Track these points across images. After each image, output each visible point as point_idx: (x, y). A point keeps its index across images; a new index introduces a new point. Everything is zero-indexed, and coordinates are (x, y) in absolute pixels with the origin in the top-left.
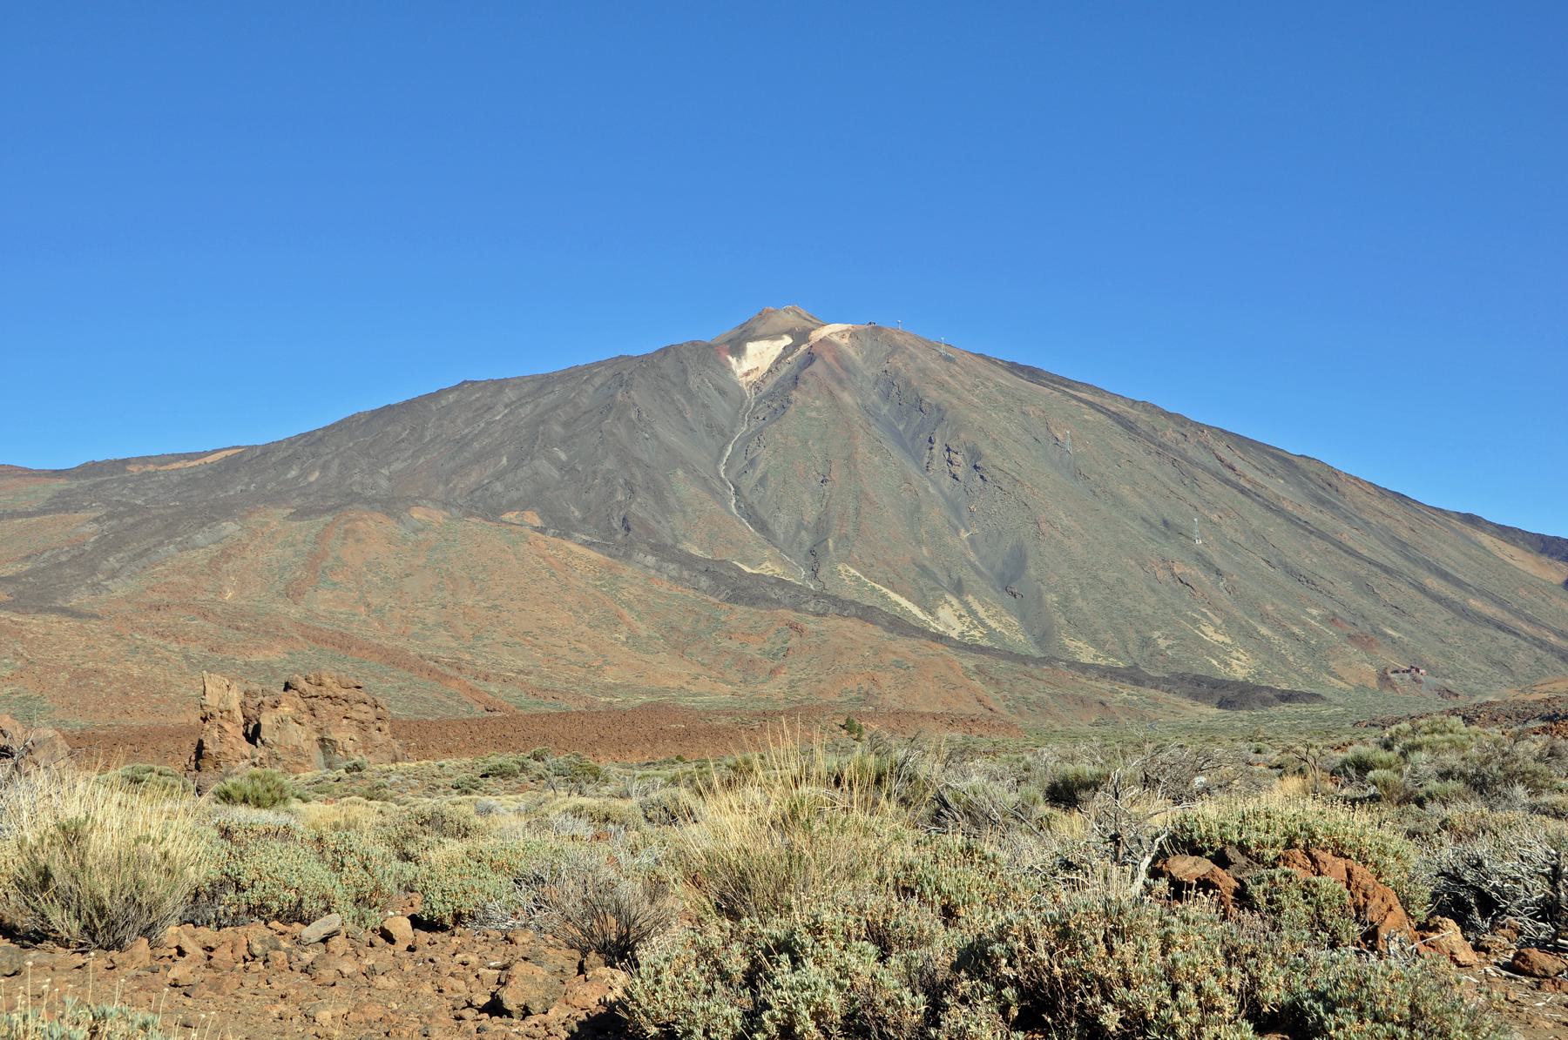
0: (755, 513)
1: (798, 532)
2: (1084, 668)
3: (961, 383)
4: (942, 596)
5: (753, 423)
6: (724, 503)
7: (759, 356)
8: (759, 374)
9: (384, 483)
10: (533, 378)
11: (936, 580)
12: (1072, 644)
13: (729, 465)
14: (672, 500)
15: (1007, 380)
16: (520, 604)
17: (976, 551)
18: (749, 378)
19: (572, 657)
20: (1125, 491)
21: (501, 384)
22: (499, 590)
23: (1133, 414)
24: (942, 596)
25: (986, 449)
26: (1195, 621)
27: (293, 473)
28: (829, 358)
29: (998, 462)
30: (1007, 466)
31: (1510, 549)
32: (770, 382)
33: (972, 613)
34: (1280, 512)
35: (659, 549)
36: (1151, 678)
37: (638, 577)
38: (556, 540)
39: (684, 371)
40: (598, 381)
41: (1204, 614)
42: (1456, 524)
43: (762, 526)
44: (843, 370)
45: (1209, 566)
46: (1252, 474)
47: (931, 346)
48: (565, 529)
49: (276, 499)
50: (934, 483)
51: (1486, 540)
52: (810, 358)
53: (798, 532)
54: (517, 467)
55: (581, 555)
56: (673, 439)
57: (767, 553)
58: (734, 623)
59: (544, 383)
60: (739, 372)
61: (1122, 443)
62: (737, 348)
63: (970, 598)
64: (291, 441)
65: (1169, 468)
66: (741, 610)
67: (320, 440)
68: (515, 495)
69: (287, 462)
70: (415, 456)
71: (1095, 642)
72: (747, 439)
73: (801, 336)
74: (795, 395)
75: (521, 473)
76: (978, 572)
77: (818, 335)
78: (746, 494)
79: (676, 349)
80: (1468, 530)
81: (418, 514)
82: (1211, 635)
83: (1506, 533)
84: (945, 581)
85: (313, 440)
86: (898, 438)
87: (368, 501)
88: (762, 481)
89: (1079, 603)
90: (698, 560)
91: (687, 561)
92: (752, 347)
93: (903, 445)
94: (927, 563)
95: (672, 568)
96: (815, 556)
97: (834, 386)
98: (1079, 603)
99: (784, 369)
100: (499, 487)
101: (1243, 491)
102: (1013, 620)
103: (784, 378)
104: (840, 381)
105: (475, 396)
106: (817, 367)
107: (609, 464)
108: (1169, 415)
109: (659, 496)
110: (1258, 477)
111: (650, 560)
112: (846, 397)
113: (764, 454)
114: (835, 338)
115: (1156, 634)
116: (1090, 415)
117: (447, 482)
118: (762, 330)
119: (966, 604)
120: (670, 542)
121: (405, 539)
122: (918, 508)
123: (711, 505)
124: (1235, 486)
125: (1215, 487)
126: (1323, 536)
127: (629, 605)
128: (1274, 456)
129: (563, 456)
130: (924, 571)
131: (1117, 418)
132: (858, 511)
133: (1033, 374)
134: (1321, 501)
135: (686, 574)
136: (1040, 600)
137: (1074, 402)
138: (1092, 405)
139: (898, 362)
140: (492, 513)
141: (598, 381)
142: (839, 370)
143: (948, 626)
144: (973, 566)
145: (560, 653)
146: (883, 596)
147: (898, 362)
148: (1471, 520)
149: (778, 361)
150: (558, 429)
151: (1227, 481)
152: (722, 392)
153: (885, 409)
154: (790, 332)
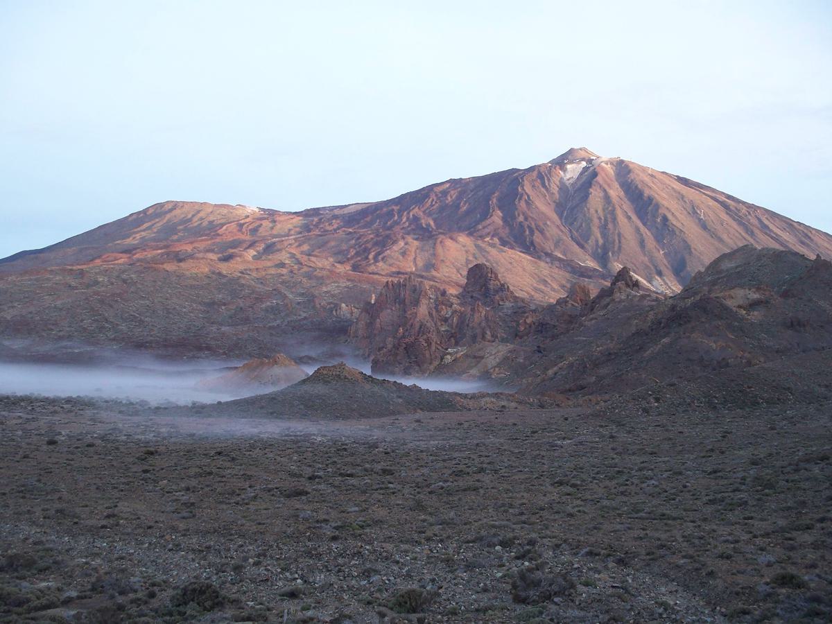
1: (597, 249)
5: (574, 202)
8: (574, 180)
14: (548, 234)
18: (571, 181)
25: (670, 216)
28: (603, 175)
29: (674, 223)
30: (679, 225)
32: (579, 183)
33: (666, 284)
43: (582, 247)
47: (644, 169)
53: (597, 249)
57: (587, 257)
63: (665, 278)
68: (487, 230)
75: (488, 222)
76: (668, 268)
84: (654, 270)
90: (563, 260)
91: (560, 260)
92: (569, 167)
94: (648, 264)
99: (584, 178)
101: (772, 238)
103: (584, 182)
104: (609, 185)
106: (599, 178)
107: (521, 218)
109: (542, 232)
111: (548, 260)
116: (712, 203)
117: (457, 224)
120: (550, 252)
122: (643, 241)
128: (785, 222)
129: (501, 214)
130: (647, 267)
131: (722, 204)
134: (803, 243)
137: (704, 196)
143: (657, 289)
144: (666, 265)
149: (581, 174)
151: (766, 234)
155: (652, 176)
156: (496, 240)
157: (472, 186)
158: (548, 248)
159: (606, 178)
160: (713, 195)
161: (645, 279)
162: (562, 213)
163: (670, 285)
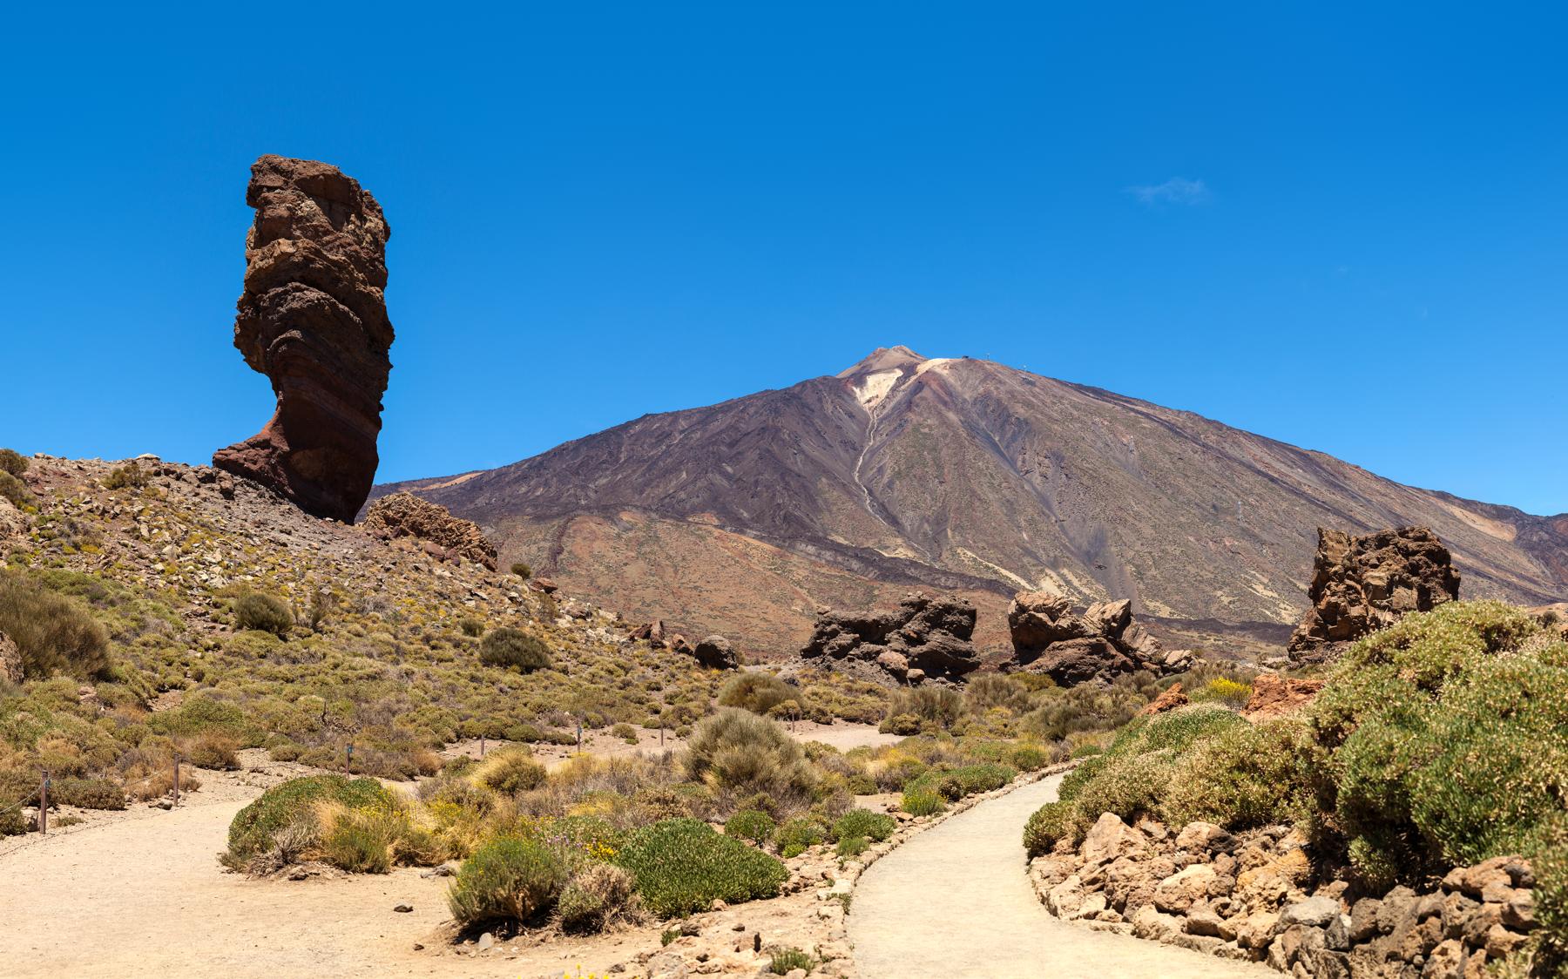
0: (885, 509)
1: (920, 526)
2: (1168, 622)
3: (1044, 403)
4: (1042, 571)
6: (859, 501)
7: (878, 388)
9: (592, 494)
10: (699, 411)
11: (1036, 558)
12: (1151, 605)
13: (862, 472)
14: (820, 501)
15: (1077, 398)
16: (716, 586)
17: (1066, 534)
19: (763, 625)
20: (1180, 482)
21: (675, 416)
22: (697, 575)
23: (1180, 420)
24: (1042, 571)
26: (1248, 581)
27: (524, 489)
31: (1473, 516)
33: (1068, 583)
34: (1302, 495)
35: (814, 540)
36: (1227, 627)
37: (802, 561)
38: (734, 536)
39: (820, 400)
40: (752, 410)
41: (1253, 576)
42: (1433, 500)
43: (894, 521)
44: (947, 396)
45: (1254, 537)
46: (1278, 466)
47: (1015, 373)
48: (740, 526)
49: (514, 509)
50: (1029, 481)
51: (1457, 511)
52: (920, 386)
53: (920, 526)
54: (695, 480)
55: (757, 548)
56: (816, 454)
57: (899, 541)
58: (887, 596)
59: (709, 414)
60: (863, 400)
61: (1175, 446)
62: (859, 379)
63: (1065, 571)
64: (518, 466)
65: (1212, 464)
66: (888, 586)
67: (541, 463)
68: (695, 500)
69: (517, 480)
70: (615, 473)
71: (1166, 603)
72: (873, 452)
73: (909, 370)
74: (911, 416)
75: (699, 484)
77: (922, 368)
78: (877, 494)
79: (812, 382)
80: (1441, 504)
81: (625, 517)
82: (1261, 591)
83: (1468, 504)
85: (536, 467)
86: (995, 446)
87: (588, 508)
88: (890, 485)
89: (1153, 572)
90: (847, 547)
91: (838, 548)
92: (871, 380)
93: (1002, 455)
95: (828, 555)
96: (936, 541)
97: (941, 406)
98: (1153, 572)
99: (900, 395)
100: (683, 495)
102: (1101, 587)
103: (899, 403)
104: (945, 404)
105: (654, 428)
106: (926, 393)
108: (1209, 422)
109: (811, 500)
110: (1284, 469)
111: (811, 549)
112: (952, 416)
113: (888, 461)
114: (938, 370)
115: (1219, 593)
116: (1146, 424)
117: (641, 492)
118: (877, 366)
119: (1063, 577)
121: (619, 536)
123: (850, 506)
124: (1266, 475)
125: (1251, 478)
126: (1337, 512)
127: (798, 583)
132: (970, 505)
133: (1099, 393)
135: (840, 559)
136: (1121, 571)
138: (1147, 416)
139: (991, 386)
140: (681, 516)
141: (752, 410)
142: (943, 395)
144: (1065, 547)
145: (755, 622)
146: (996, 572)
147: (991, 386)
148: (1443, 496)
149: (894, 389)
150: (723, 448)
152: (851, 416)
153: (983, 424)
154: (900, 367)
155: (1029, 383)
156: (710, 519)
157: (683, 424)
158: (818, 526)
159: (941, 392)
160: (1151, 412)
161: (1024, 577)
162: (856, 459)
163: (1076, 582)
